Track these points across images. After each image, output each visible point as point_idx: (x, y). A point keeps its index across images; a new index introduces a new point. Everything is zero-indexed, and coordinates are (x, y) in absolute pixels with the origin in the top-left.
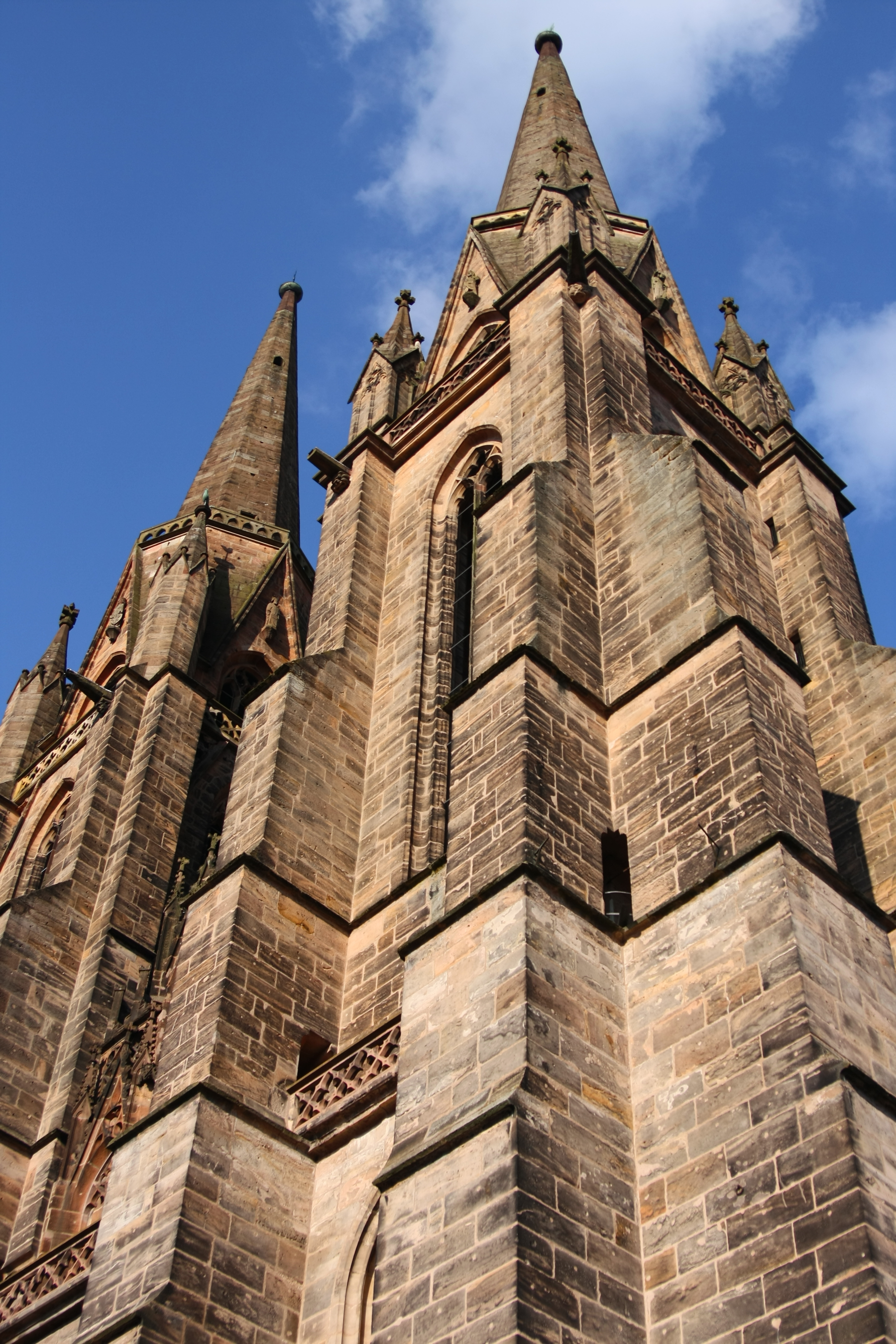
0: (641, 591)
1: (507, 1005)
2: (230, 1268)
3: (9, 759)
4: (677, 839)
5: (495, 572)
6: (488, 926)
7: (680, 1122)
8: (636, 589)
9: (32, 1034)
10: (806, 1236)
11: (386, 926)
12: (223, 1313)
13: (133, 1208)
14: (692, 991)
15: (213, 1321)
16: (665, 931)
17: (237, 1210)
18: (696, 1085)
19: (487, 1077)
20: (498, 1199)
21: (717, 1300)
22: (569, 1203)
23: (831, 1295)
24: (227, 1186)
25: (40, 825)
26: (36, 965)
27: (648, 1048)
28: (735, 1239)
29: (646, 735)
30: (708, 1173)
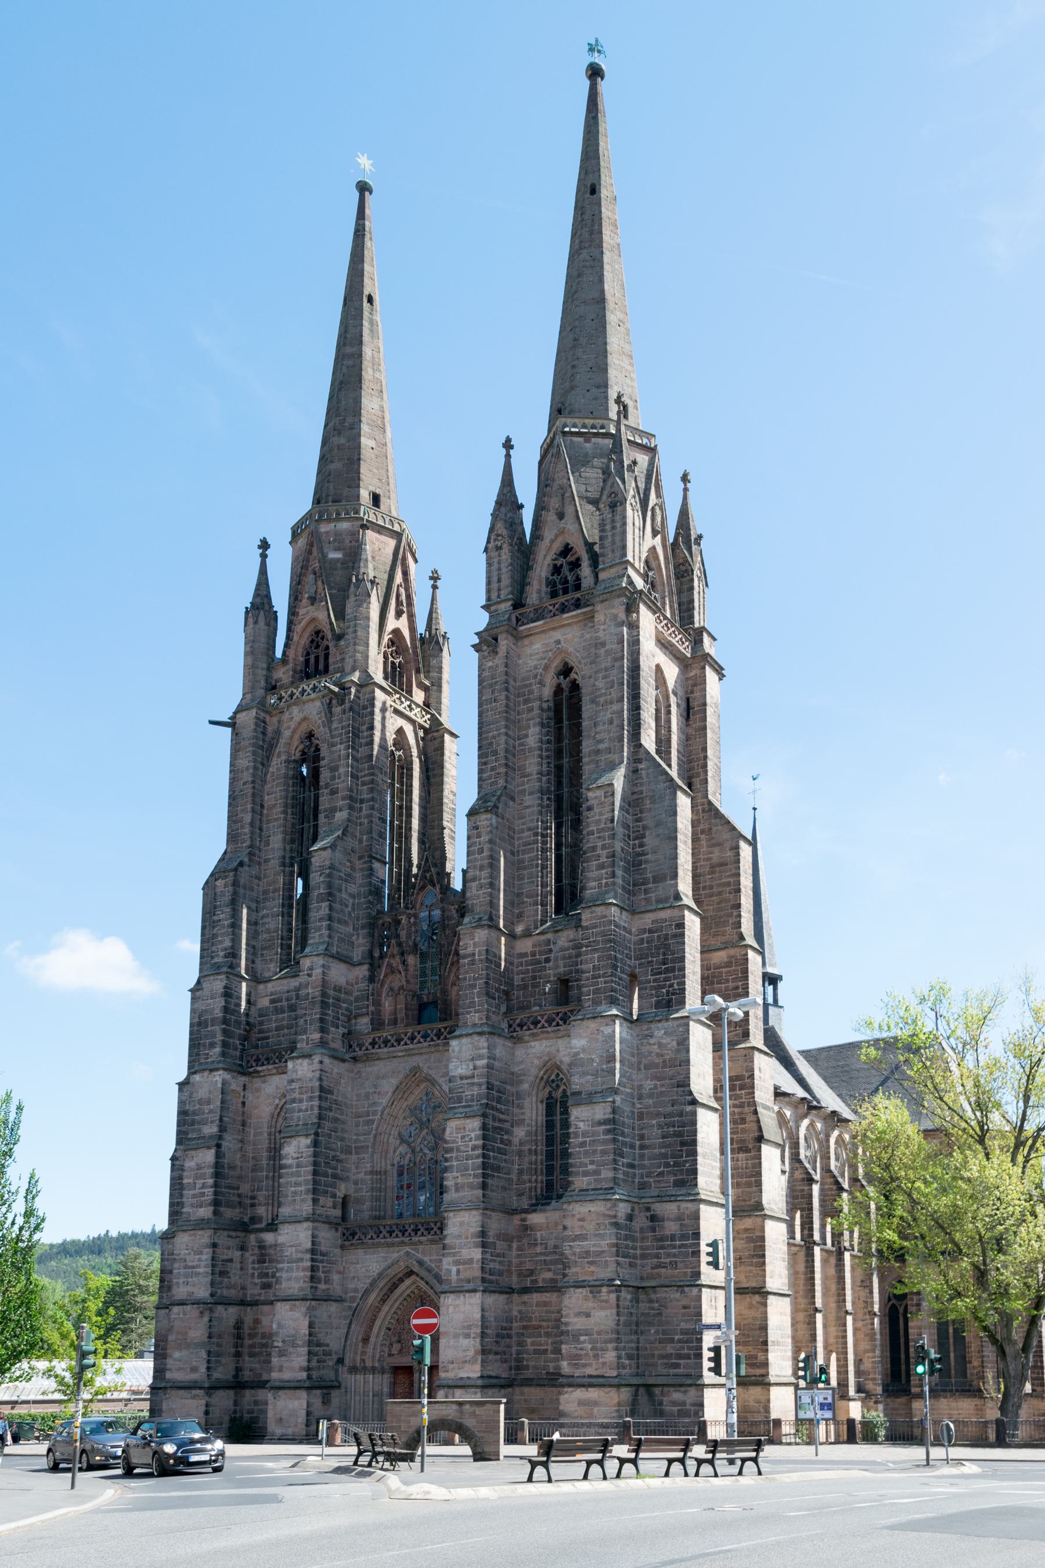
0: (649, 856)
4: (655, 988)
7: (650, 1096)
8: (647, 854)
10: (683, 1144)
11: (534, 946)
12: (499, 1106)
15: (497, 1110)
16: (649, 1029)
18: (656, 1087)
19: (603, 1083)
20: (608, 1127)
21: (657, 1151)
22: (624, 1123)
23: (686, 1161)
24: (496, 1064)
27: (642, 1067)
28: (663, 1137)
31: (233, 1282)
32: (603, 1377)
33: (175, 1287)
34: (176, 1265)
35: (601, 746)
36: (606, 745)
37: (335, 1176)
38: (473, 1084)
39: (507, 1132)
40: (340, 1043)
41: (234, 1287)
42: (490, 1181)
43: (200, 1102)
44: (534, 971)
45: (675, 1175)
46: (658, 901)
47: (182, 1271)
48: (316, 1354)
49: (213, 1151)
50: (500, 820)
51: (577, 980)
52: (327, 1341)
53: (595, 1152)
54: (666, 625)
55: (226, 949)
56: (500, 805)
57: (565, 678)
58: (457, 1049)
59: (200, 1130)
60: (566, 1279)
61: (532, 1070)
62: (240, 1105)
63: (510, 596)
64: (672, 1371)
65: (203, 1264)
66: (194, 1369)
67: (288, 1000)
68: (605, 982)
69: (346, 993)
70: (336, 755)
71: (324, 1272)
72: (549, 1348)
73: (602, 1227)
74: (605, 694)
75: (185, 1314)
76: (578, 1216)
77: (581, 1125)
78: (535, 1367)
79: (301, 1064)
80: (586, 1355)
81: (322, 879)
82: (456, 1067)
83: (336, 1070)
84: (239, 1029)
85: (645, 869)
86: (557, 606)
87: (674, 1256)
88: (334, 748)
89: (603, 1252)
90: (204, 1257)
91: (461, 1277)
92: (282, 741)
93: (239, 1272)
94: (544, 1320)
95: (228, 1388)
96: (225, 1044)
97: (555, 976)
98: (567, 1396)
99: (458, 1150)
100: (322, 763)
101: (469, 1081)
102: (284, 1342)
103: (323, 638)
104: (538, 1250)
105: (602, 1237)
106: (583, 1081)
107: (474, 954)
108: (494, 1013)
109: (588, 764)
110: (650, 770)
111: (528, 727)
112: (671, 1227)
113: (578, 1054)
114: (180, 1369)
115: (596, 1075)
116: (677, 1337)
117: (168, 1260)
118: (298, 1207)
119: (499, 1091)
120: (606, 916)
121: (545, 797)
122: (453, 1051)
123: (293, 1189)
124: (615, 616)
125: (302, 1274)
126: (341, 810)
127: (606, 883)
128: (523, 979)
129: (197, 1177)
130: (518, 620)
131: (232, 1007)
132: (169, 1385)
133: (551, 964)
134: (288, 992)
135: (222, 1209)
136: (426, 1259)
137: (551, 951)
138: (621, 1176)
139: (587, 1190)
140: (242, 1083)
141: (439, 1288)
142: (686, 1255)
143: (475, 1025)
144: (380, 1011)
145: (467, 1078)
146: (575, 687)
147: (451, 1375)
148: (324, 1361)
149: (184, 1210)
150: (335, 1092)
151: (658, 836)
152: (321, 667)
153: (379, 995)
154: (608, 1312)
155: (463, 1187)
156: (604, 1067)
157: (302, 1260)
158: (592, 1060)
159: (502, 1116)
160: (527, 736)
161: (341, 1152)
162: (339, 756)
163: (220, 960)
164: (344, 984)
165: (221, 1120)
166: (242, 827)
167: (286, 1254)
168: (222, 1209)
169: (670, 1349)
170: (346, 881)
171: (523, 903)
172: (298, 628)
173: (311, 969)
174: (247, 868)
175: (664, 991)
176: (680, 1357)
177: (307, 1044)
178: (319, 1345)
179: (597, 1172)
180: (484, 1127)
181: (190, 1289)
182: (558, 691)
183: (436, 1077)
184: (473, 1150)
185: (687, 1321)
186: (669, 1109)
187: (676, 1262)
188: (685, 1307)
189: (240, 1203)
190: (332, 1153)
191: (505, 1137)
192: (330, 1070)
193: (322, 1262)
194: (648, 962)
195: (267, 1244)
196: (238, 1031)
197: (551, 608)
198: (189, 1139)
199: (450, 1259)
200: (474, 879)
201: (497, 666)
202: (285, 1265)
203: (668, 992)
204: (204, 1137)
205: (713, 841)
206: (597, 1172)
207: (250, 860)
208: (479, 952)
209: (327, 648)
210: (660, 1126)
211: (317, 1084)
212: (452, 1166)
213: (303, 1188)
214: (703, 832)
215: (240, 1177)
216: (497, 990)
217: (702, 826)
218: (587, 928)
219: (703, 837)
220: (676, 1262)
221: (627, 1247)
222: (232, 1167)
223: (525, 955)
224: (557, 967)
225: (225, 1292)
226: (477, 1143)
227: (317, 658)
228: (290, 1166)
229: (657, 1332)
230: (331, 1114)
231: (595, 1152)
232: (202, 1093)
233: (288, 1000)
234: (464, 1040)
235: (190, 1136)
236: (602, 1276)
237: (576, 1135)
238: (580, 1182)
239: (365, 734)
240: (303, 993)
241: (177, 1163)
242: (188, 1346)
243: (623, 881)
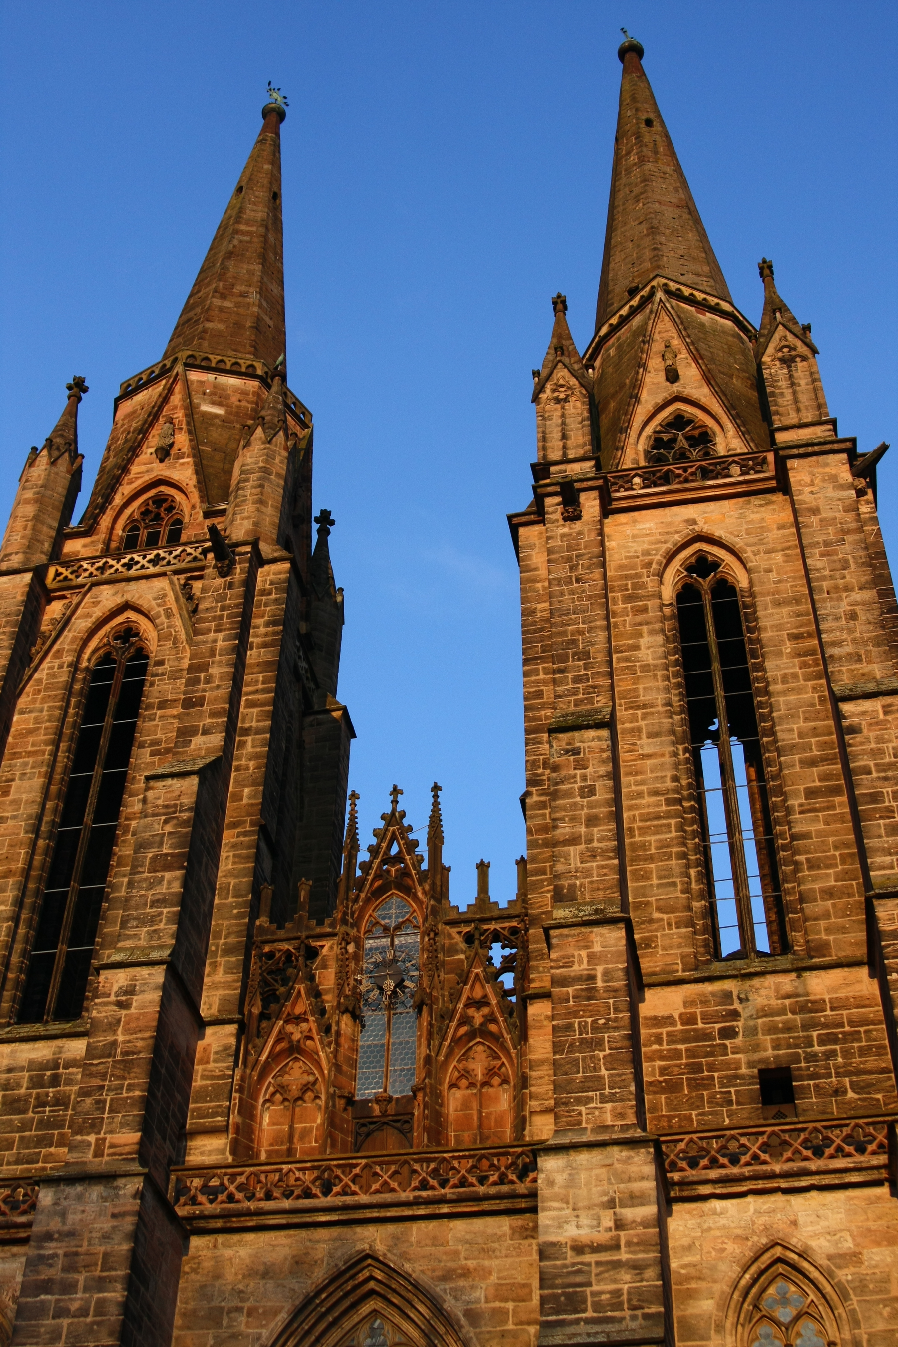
3: (42, 537)
5: (874, 775)
11: (686, 1004)
25: (92, 632)
44: (691, 1053)
51: (814, 1076)
58: (560, 1179)
70: (204, 648)
74: (831, 577)
79: (80, 1198)
81: (168, 828)
92: (68, 635)
97: (750, 1065)
101: (604, 1257)
107: (592, 978)
109: (784, 693)
111: (640, 635)
121: (681, 747)
122: (551, 1183)
126: (205, 732)
128: (663, 1071)
133: (739, 1040)
134: (10, 1070)
137: (735, 1015)
143: (605, 1128)
153: (254, 1096)
160: (637, 647)
171: (651, 921)
173: (130, 991)
177: (98, 1153)
201: (580, 533)
208: (606, 973)
211: (126, 1247)
223: (668, 1020)
224: (756, 1048)
239: (262, 630)
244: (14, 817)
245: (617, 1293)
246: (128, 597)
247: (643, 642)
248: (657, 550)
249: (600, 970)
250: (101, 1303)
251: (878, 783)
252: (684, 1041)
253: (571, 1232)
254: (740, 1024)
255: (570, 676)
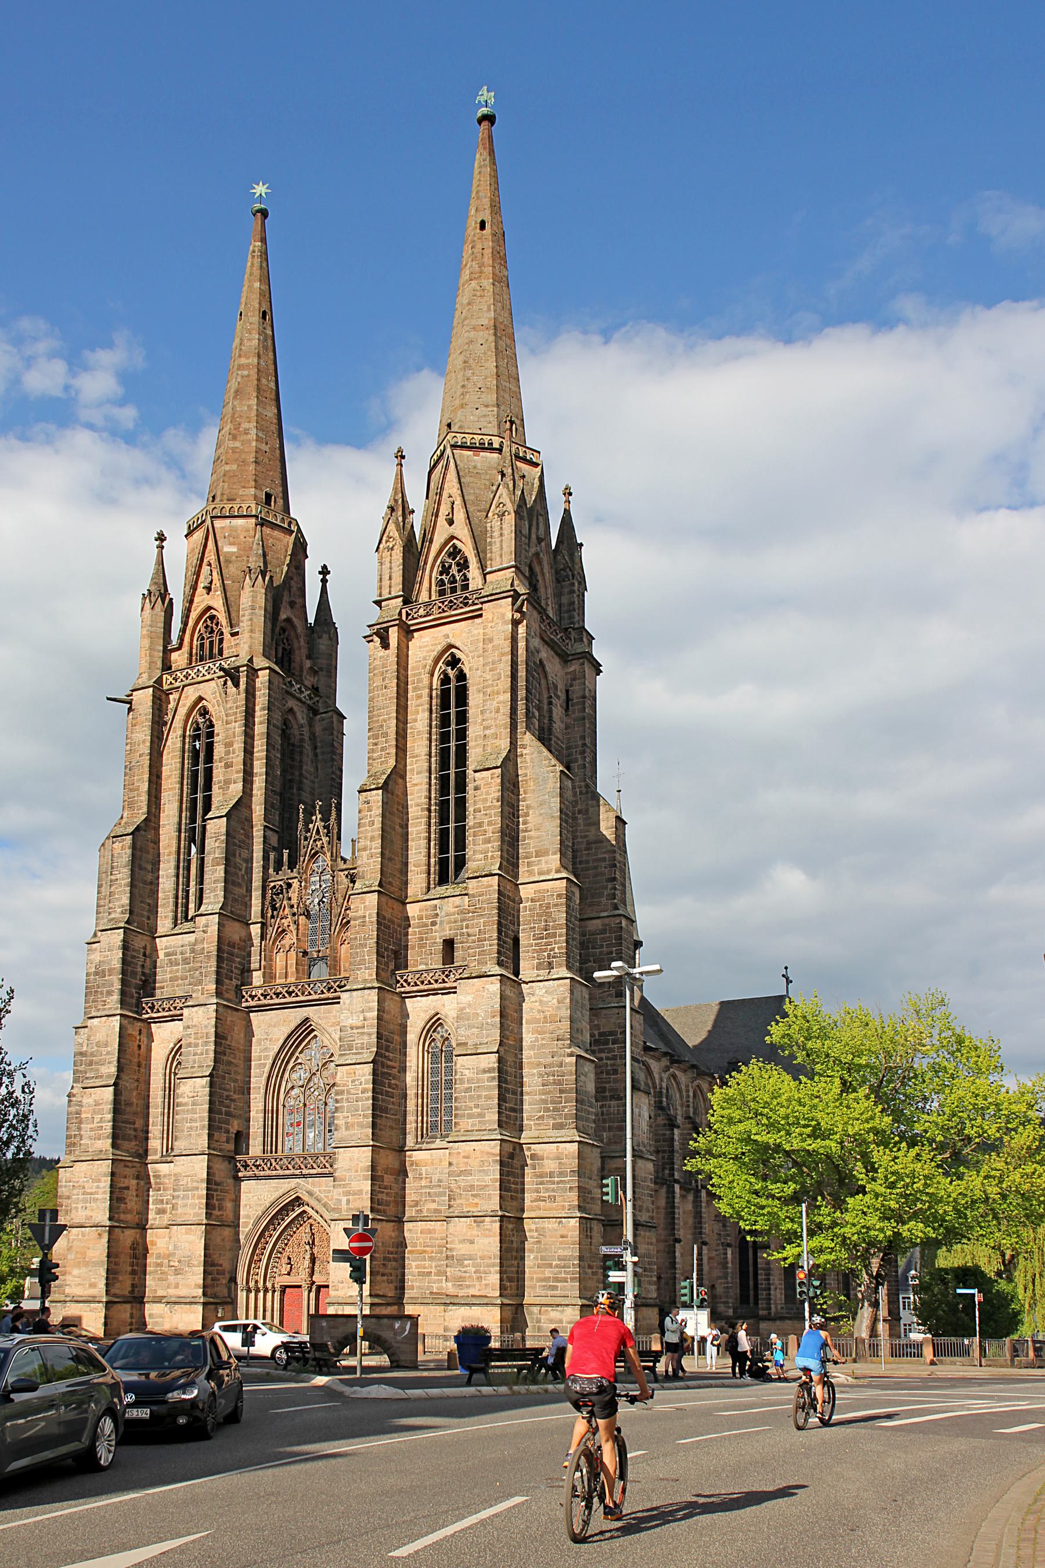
0: (532, 833)
1: (494, 1017)
2: (387, 1041)
6: (487, 986)
9: (240, 873)
10: (561, 1091)
12: (387, 1054)
13: (354, 1018)
14: (539, 1011)
15: (386, 1057)
17: (387, 1022)
18: (537, 1040)
21: (537, 1097)
22: (507, 1072)
26: (237, 842)
29: (530, 903)
30: (539, 1065)
31: (129, 1208)
32: (486, 1296)
33: (74, 1211)
34: (75, 1192)
35: (487, 732)
36: (492, 731)
37: (228, 1114)
38: (363, 1033)
39: (394, 1078)
40: (233, 993)
41: (130, 1212)
42: (378, 1121)
43: (98, 1044)
45: (555, 1119)
46: (540, 874)
47: (81, 1197)
48: (210, 1274)
49: (112, 1089)
50: (390, 795)
52: (220, 1262)
53: (479, 1097)
54: (549, 624)
55: (123, 906)
56: (390, 783)
57: (452, 669)
58: (347, 1002)
59: (98, 1070)
60: (451, 1210)
61: (419, 1022)
62: (136, 1048)
63: (401, 593)
64: (550, 1293)
65: (101, 1191)
66: (93, 1285)
67: (182, 953)
68: (490, 945)
69: (239, 948)
71: (217, 1200)
72: (433, 1270)
73: (486, 1164)
75: (83, 1235)
76: (462, 1154)
77: (466, 1072)
78: (419, 1288)
80: (470, 1277)
81: (217, 844)
82: (347, 1018)
83: (229, 1019)
84: (136, 979)
85: (529, 844)
86: (446, 603)
87: (553, 1190)
88: (229, 726)
89: (487, 1186)
90: (102, 1185)
91: (351, 1206)
93: (135, 1199)
94: (428, 1246)
95: (125, 1302)
96: (123, 993)
98: (451, 1313)
99: (348, 1093)
100: (216, 739)
101: (360, 1031)
102: (179, 1261)
103: (217, 624)
104: (423, 1183)
105: (486, 1172)
106: (468, 1033)
107: (365, 917)
108: (383, 970)
110: (533, 756)
112: (550, 1165)
113: (465, 1008)
114: (80, 1284)
115: (481, 1028)
116: (554, 1263)
117: (66, 1186)
118: (193, 1141)
119: (387, 1041)
120: (492, 886)
123: (188, 1125)
124: (503, 615)
125: (197, 1201)
127: (492, 856)
129: (94, 1112)
130: (408, 615)
131: (129, 959)
132: (68, 1299)
135: (119, 1142)
136: (316, 1190)
138: (504, 1119)
139: (472, 1131)
140: (138, 1029)
141: (327, 1216)
142: (564, 1190)
144: (271, 966)
145: (357, 1028)
146: (462, 676)
147: (341, 1293)
148: (218, 1280)
149: (82, 1142)
150: (229, 1038)
151: (541, 814)
152: (216, 650)
154: (491, 1239)
155: (353, 1125)
156: (489, 1021)
157: (197, 1188)
158: (478, 1014)
159: (390, 1063)
161: (235, 1093)
162: (234, 734)
163: (117, 915)
164: (238, 941)
165: (119, 1061)
166: (139, 795)
167: (181, 1183)
168: (119, 1142)
169: (548, 1272)
170: (240, 847)
172: (193, 616)
173: (207, 926)
174: (142, 832)
175: (546, 954)
176: (557, 1280)
177: (202, 994)
178: (213, 1265)
179: (481, 1115)
180: (375, 1073)
181: (88, 1213)
182: (445, 680)
183: (325, 1027)
184: (362, 1093)
185: (564, 1249)
186: (549, 1060)
187: (555, 1197)
188: (562, 1237)
189: (135, 1136)
190: (226, 1093)
191: (393, 1082)
192: (224, 1019)
193: (216, 1190)
194: (531, 928)
195: (162, 1174)
196: (134, 981)
197: (440, 605)
198: (87, 1078)
199: (341, 1190)
200: (365, 849)
202: (181, 1193)
203: (549, 956)
204: (102, 1077)
205: (589, 821)
206: (481, 1115)
207: (146, 825)
209: (222, 634)
210: (540, 1075)
212: (343, 1106)
213: (198, 1124)
214: (580, 812)
215: (135, 1113)
216: (386, 949)
217: (579, 807)
218: (473, 896)
219: (580, 816)
220: (555, 1196)
221: (509, 1182)
222: (130, 1104)
225: (122, 1217)
226: (367, 1086)
227: (211, 643)
228: (186, 1104)
229: (536, 1258)
230: (225, 1058)
231: (479, 1097)
232: (100, 1036)
233: (182, 953)
234: (355, 993)
235: (88, 1075)
236: (485, 1208)
237: (462, 1081)
238: (465, 1124)
240: (198, 947)
241: (74, 1099)
242: (87, 1264)
243: (508, 854)
244: (168, 824)
245: (363, 1044)
246: (200, 693)
247: (419, 717)
248: (429, 656)
249: (368, 913)
250: (207, 1050)
251: (483, 817)
252: (418, 927)
253: (350, 1021)
254: (438, 920)
255: (379, 747)
